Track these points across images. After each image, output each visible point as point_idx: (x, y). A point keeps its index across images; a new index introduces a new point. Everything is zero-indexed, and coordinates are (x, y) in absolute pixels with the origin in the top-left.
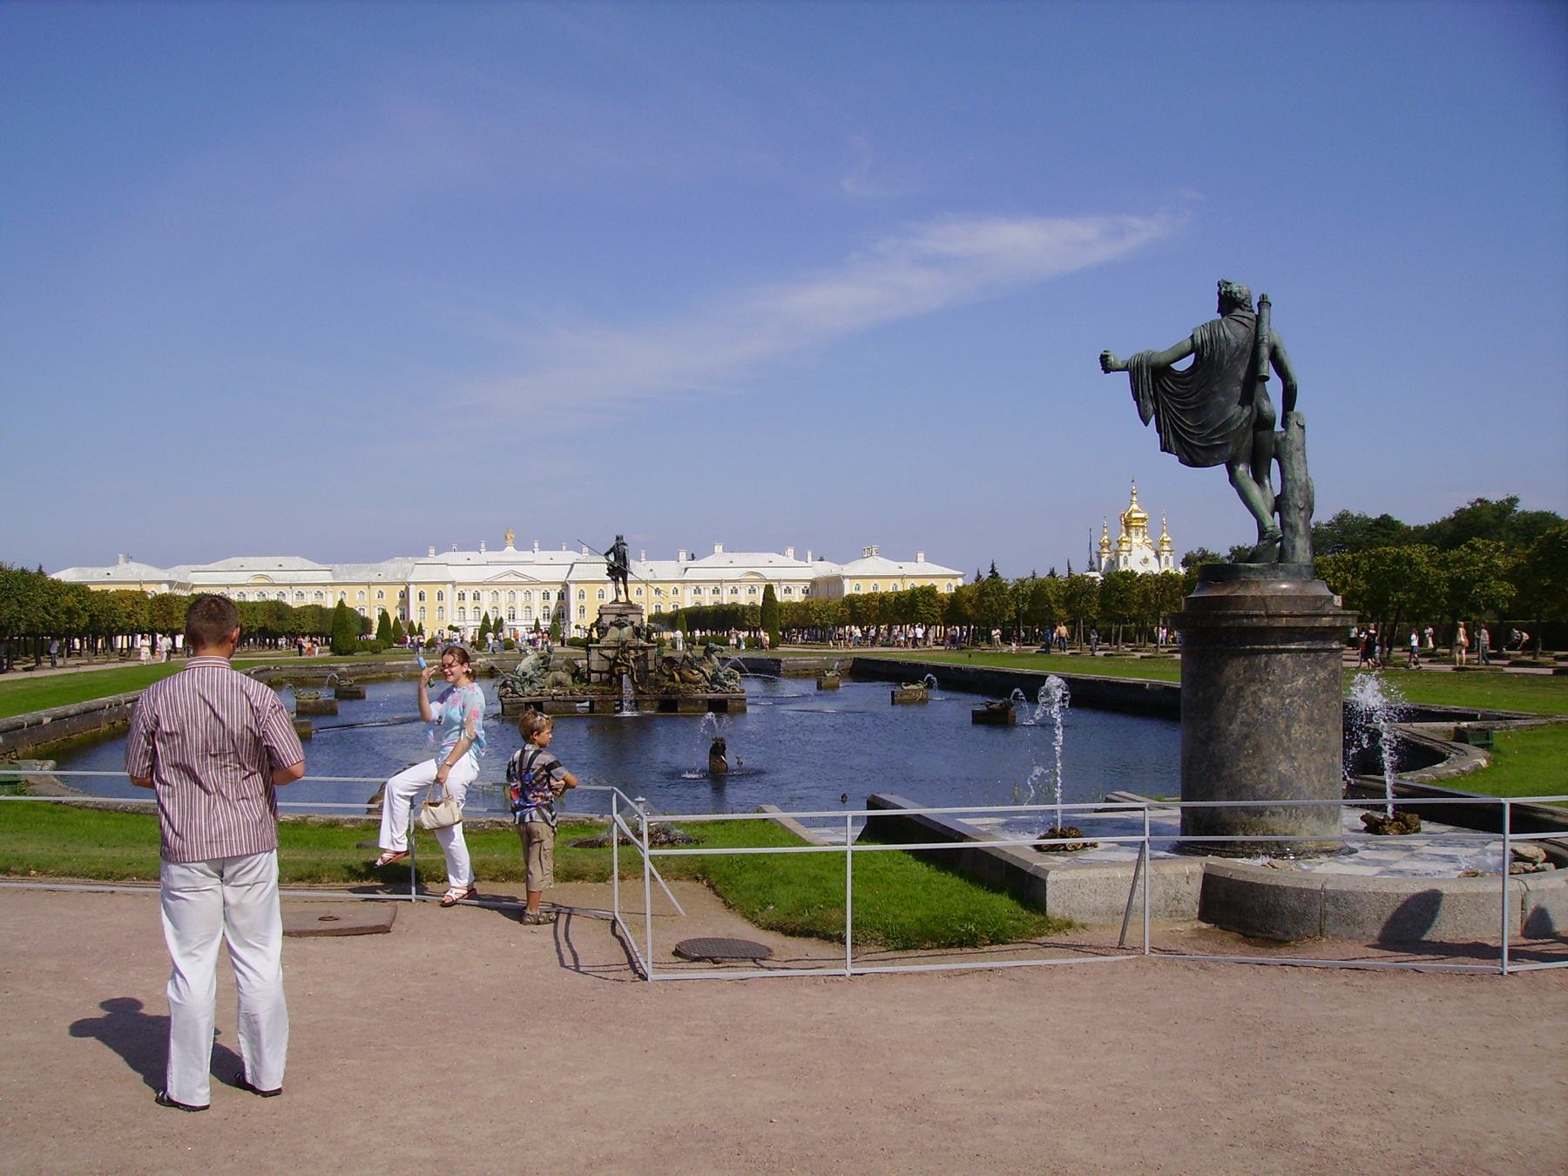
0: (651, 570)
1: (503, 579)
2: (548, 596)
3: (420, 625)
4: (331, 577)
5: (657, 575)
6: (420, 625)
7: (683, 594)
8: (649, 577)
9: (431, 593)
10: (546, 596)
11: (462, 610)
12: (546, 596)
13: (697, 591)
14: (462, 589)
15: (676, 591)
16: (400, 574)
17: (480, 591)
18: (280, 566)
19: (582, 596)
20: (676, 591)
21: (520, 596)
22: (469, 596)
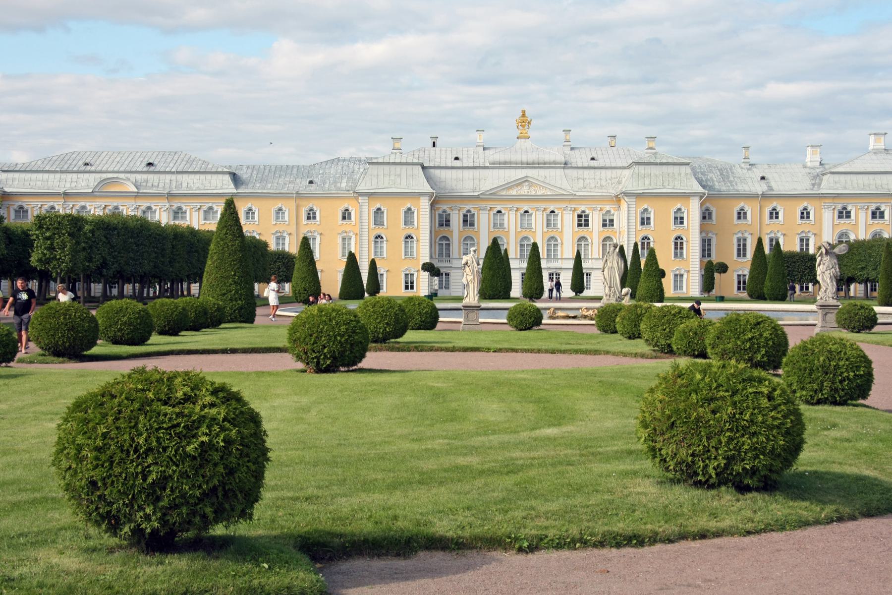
0: (763, 178)
1: (514, 192)
2: (587, 221)
3: (373, 265)
4: (232, 186)
5: (773, 184)
6: (373, 265)
7: (819, 220)
8: (760, 188)
9: (394, 213)
10: (583, 220)
11: (444, 242)
12: (583, 220)
13: (844, 214)
14: (445, 207)
15: (805, 214)
16: (345, 181)
17: (473, 211)
18: (150, 164)
19: (645, 221)
20: (805, 214)
21: (538, 220)
22: (456, 220)
